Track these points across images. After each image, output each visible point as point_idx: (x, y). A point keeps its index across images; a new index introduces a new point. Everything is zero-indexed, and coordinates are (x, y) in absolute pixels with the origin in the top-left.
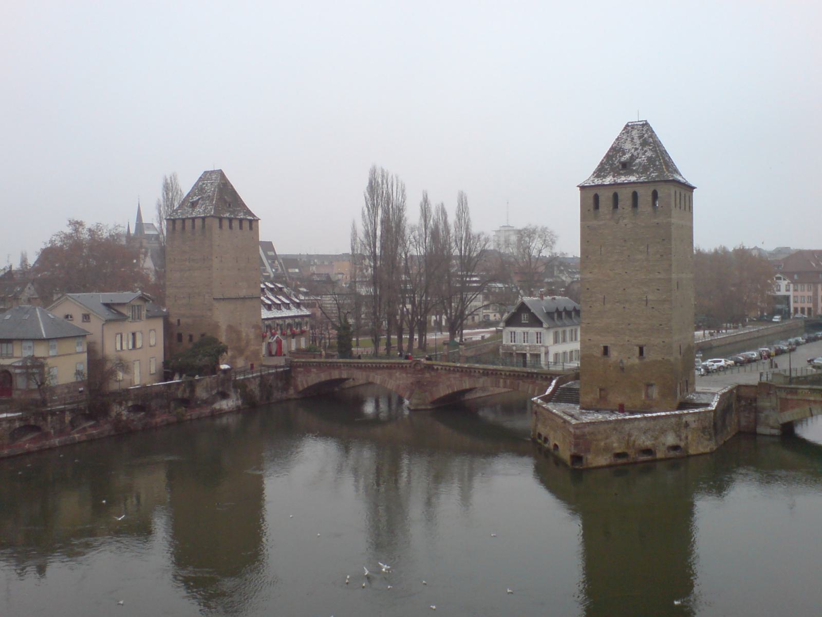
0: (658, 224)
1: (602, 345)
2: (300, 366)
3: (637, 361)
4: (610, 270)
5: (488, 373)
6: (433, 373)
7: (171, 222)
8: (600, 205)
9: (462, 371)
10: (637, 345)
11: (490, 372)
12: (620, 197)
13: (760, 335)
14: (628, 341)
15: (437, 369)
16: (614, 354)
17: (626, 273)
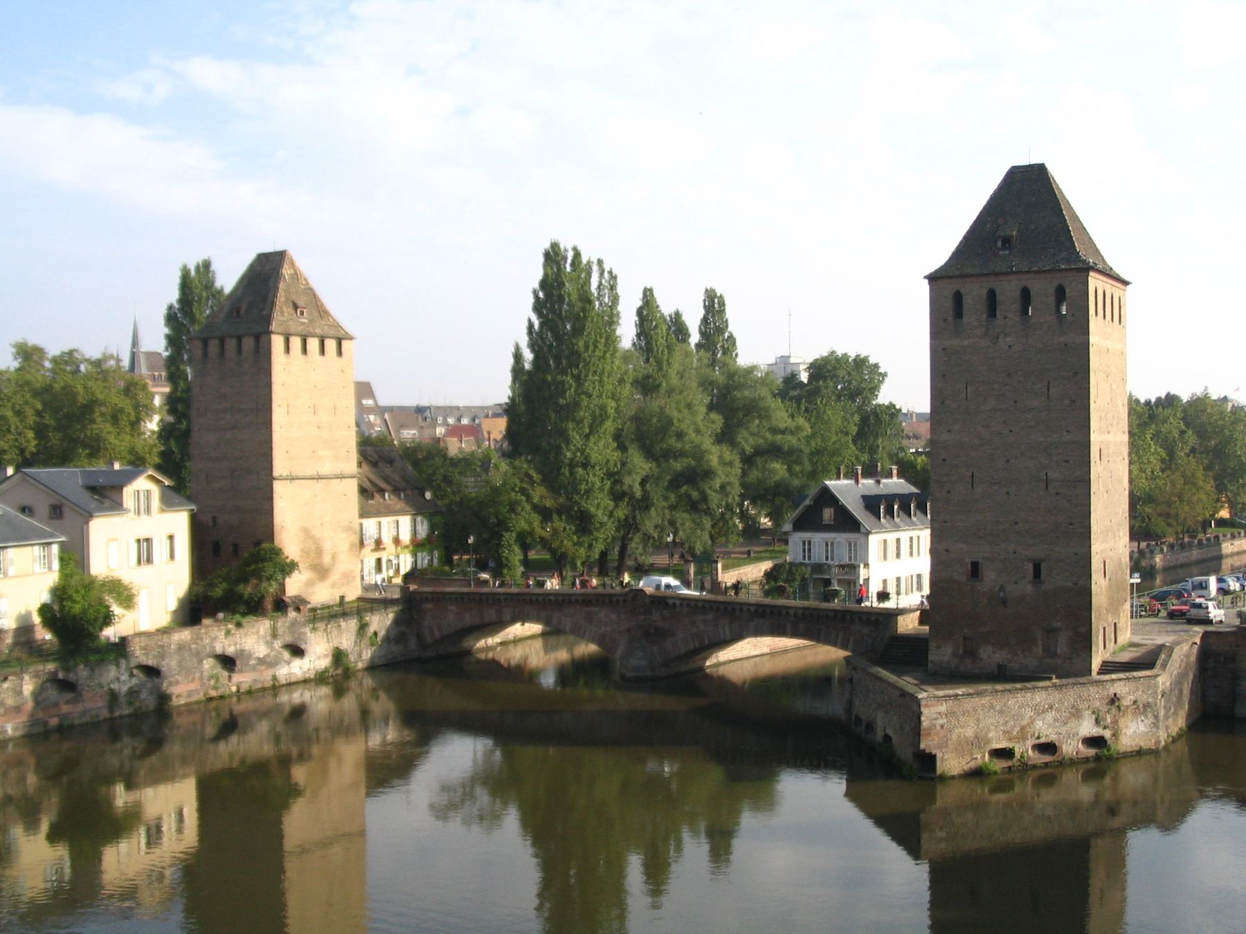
0: (1066, 345)
1: (968, 560)
2: (427, 600)
3: (1029, 588)
4: (983, 426)
5: (764, 612)
6: (666, 613)
7: (199, 344)
8: (964, 312)
9: (718, 608)
10: (1030, 560)
11: (768, 611)
12: (999, 298)
13: (1236, 550)
14: (1015, 553)
15: (674, 604)
16: (990, 576)
17: (1011, 431)
